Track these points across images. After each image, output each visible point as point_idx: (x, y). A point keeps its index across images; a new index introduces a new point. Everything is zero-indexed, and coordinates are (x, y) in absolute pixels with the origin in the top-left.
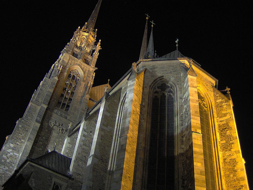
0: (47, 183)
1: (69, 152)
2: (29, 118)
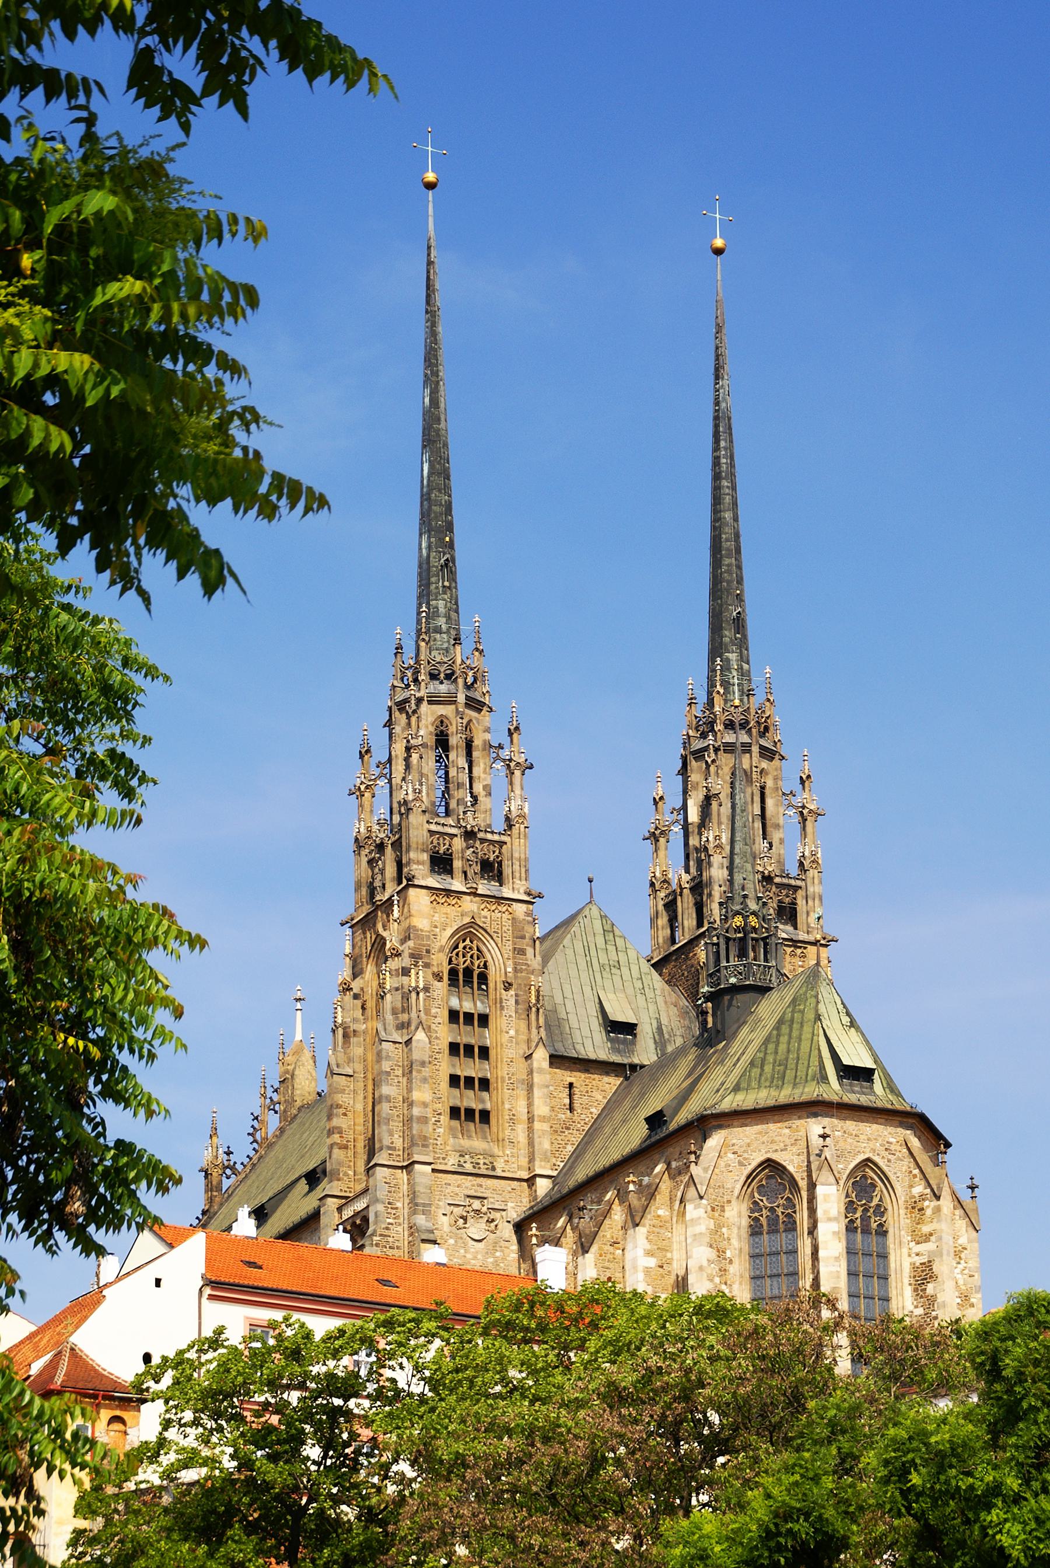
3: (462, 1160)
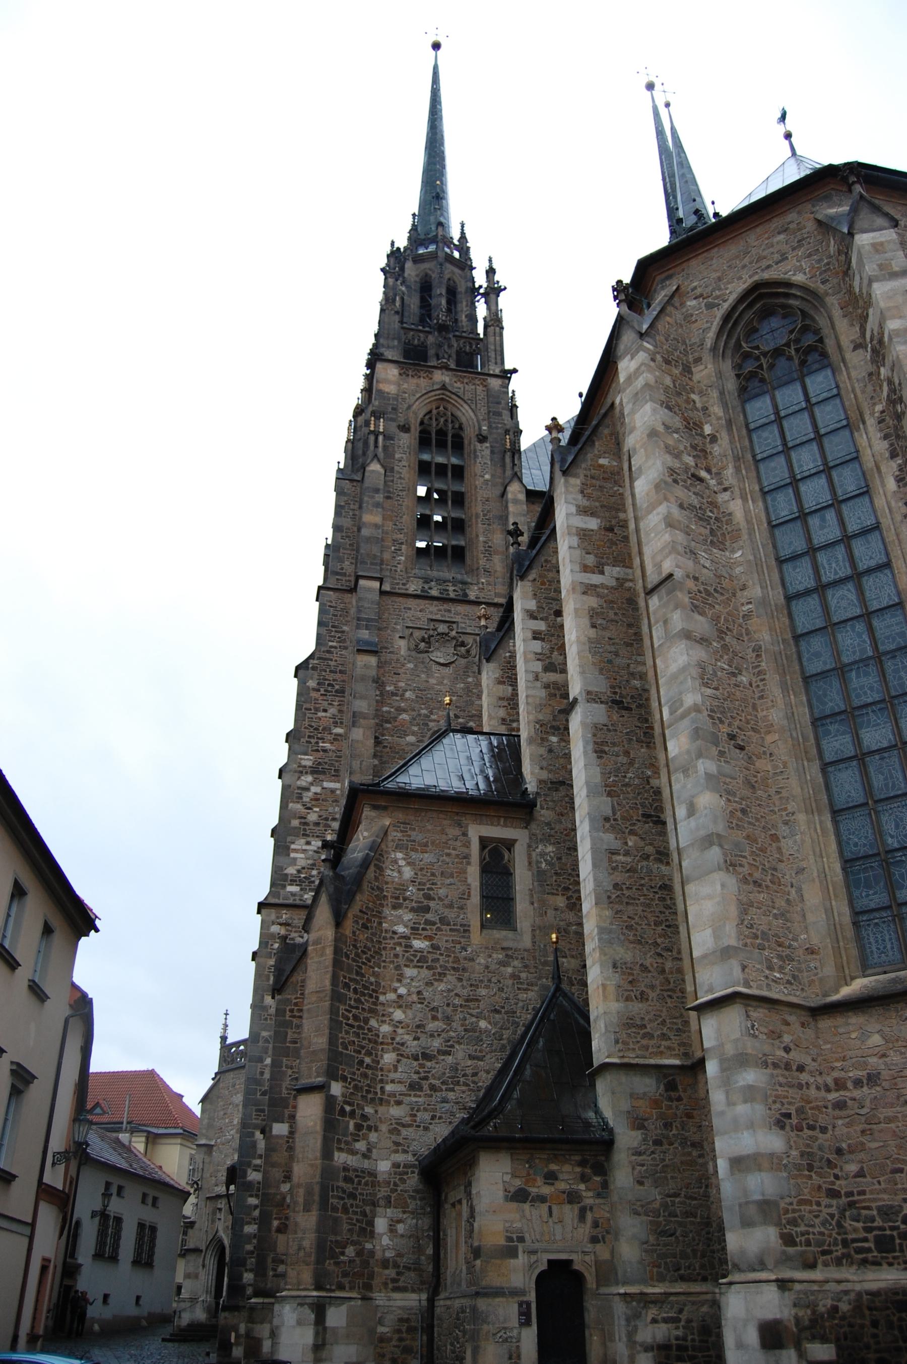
0: (453, 852)
1: (509, 714)
2: (331, 647)
3: (426, 587)
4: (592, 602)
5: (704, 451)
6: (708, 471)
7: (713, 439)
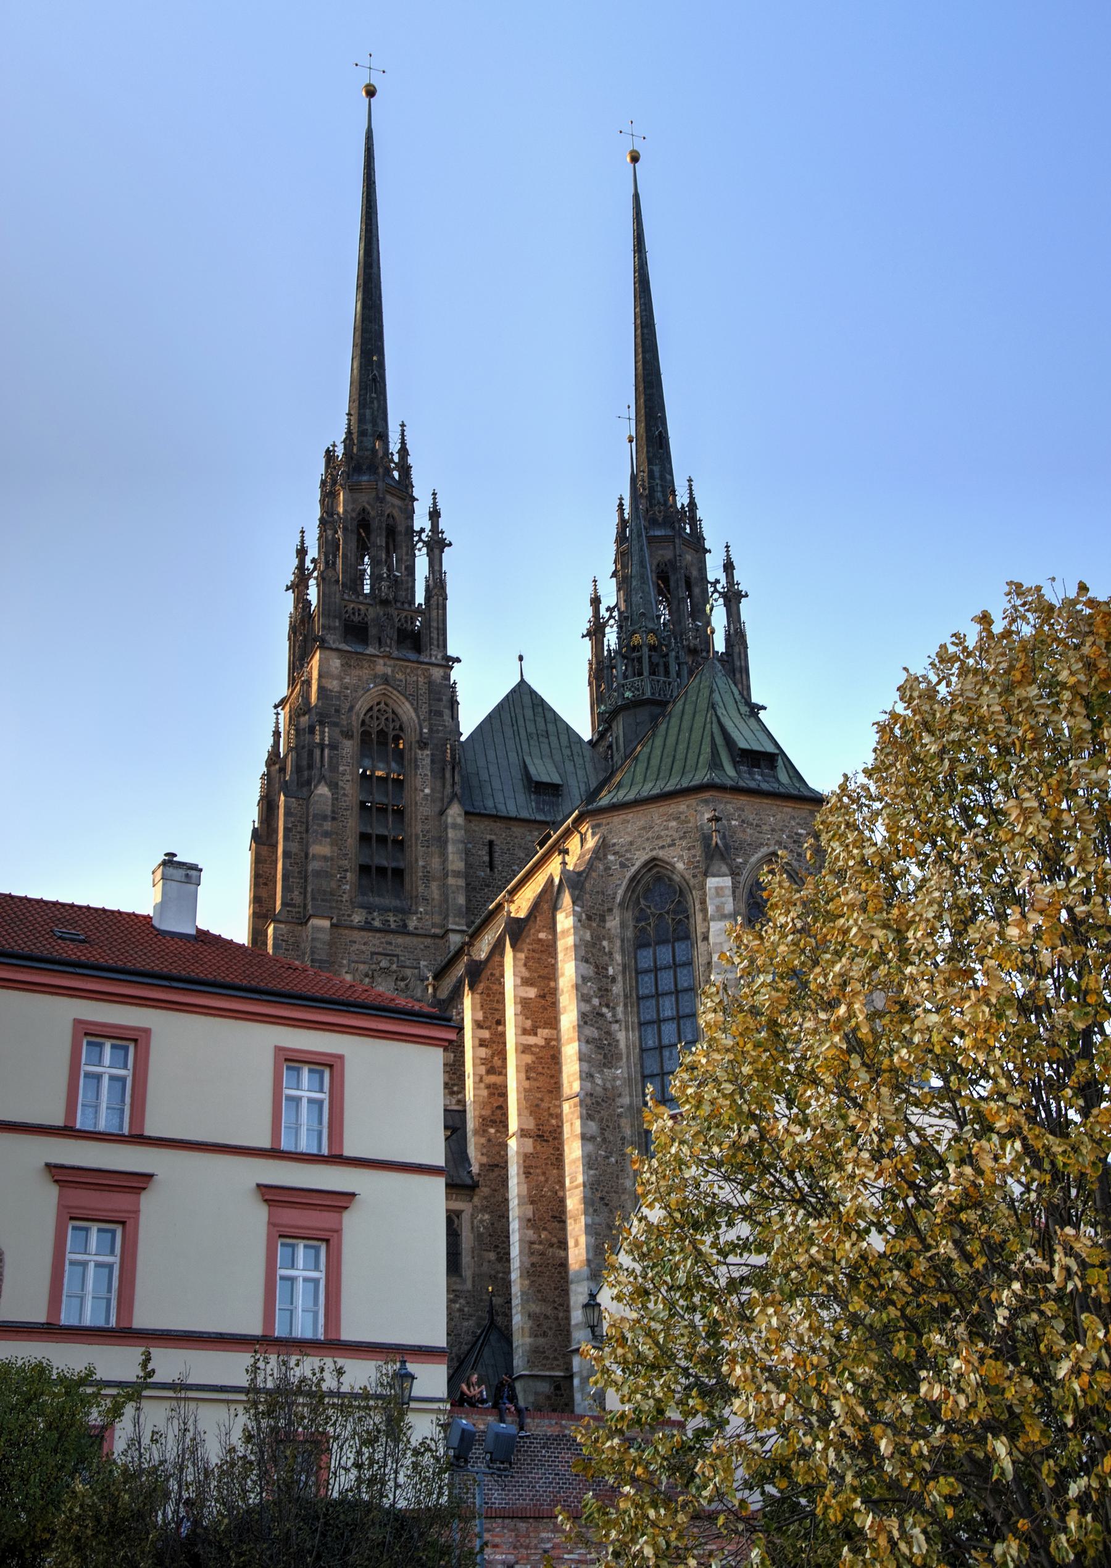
1: (450, 1078)
4: (528, 1059)
5: (606, 990)
6: (607, 1006)
7: (614, 980)
